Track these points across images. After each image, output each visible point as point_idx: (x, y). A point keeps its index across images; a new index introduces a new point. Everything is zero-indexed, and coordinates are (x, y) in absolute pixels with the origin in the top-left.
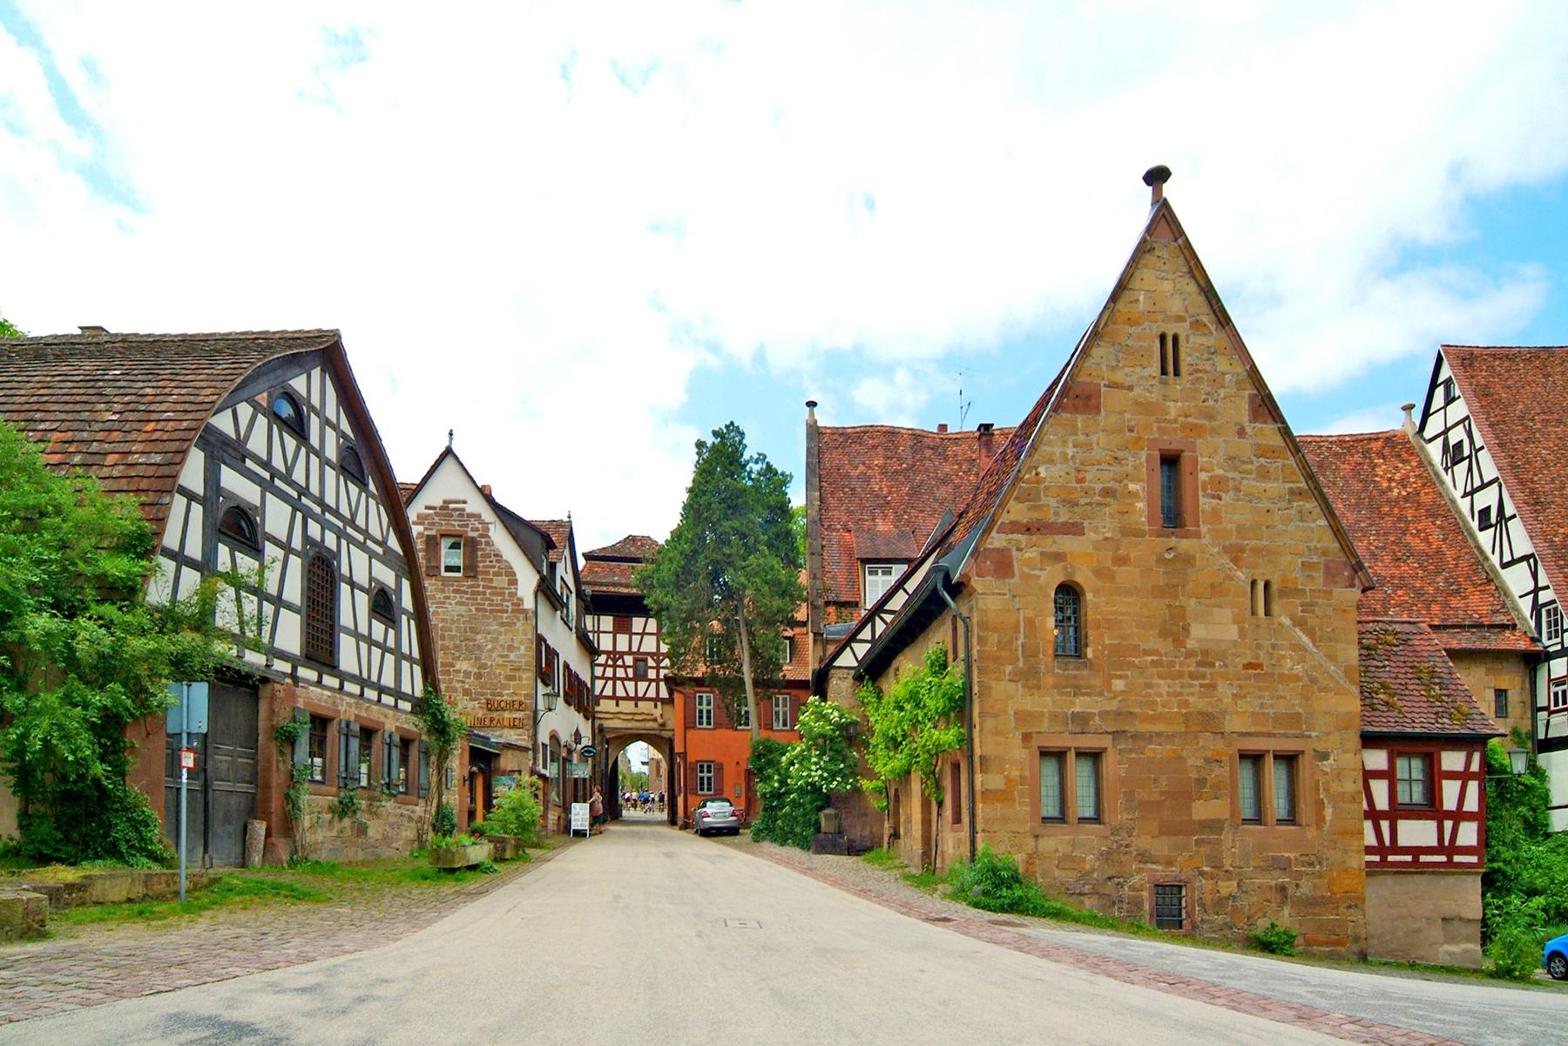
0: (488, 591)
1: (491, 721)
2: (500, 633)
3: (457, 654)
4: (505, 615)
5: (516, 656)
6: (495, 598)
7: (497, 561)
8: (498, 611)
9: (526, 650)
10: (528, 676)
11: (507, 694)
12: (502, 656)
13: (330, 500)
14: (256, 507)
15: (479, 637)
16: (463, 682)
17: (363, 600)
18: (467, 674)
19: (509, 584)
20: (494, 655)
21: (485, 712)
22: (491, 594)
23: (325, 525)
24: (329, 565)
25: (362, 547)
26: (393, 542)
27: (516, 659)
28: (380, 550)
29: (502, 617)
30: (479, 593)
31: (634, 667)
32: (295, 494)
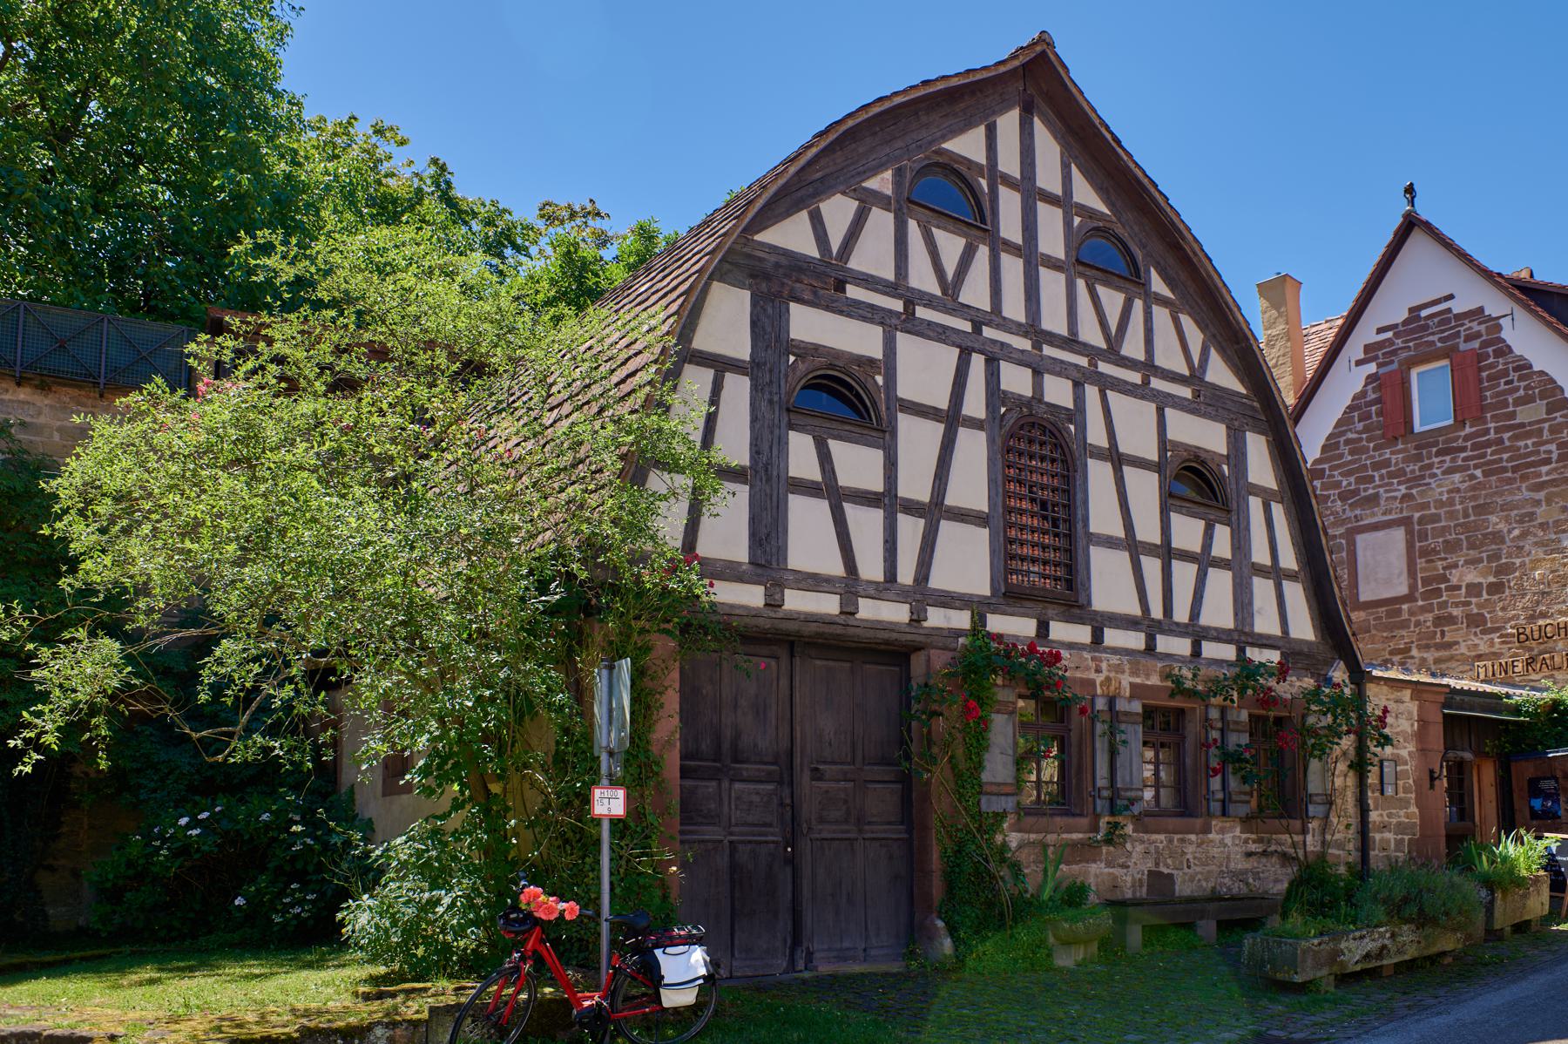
0: (1506, 436)
2: (1538, 503)
4: (1544, 469)
6: (1522, 443)
7: (1521, 379)
15: (1493, 519)
16: (1468, 604)
18: (1474, 589)
19: (1547, 414)
20: (1528, 544)
30: (1488, 444)
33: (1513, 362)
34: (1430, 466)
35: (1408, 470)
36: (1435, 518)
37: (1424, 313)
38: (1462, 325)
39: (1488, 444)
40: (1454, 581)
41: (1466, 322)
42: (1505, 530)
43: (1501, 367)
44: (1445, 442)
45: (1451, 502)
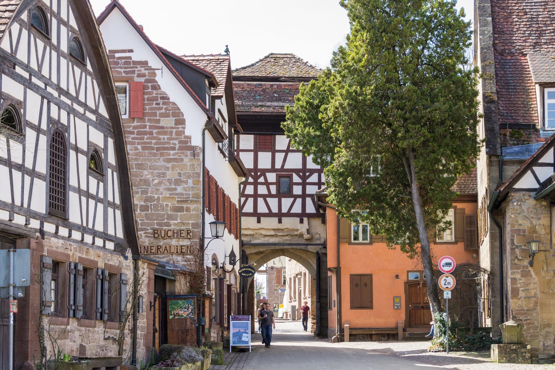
0: (155, 131)
2: (168, 168)
4: (172, 152)
6: (162, 137)
7: (163, 104)
9: (194, 184)
10: (197, 207)
12: (169, 189)
13: (63, 86)
14: (21, 102)
15: (145, 172)
17: (83, 160)
19: (176, 124)
20: (161, 189)
23: (60, 106)
24: (63, 138)
25: (83, 117)
26: (103, 111)
27: (184, 192)
28: (93, 117)
30: (145, 133)
31: (278, 184)
32: (42, 85)
33: (161, 94)
37: (117, 55)
38: (137, 68)
39: (145, 133)
41: (139, 66)
42: (151, 179)
43: (154, 95)
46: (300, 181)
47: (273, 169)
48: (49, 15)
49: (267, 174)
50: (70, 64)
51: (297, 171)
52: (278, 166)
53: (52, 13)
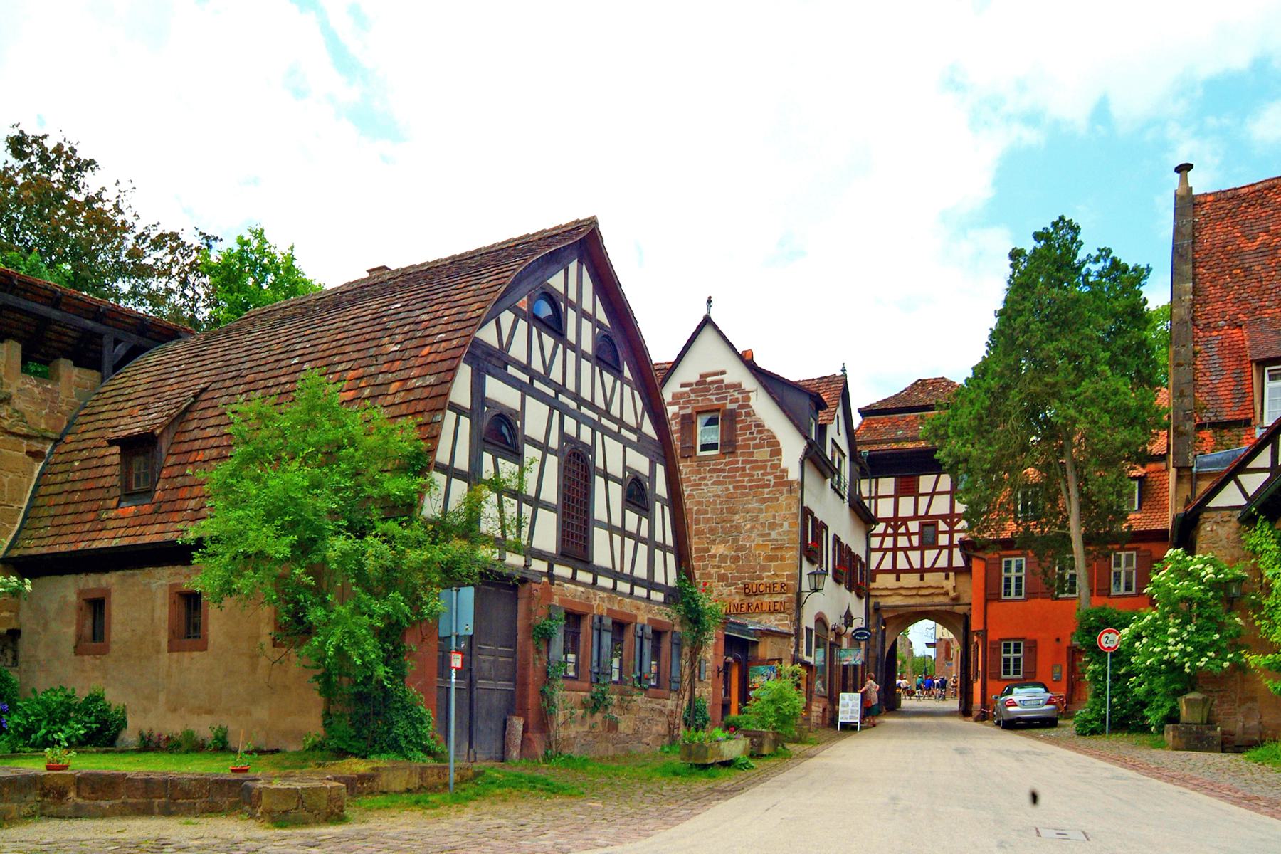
0: (748, 466)
1: (749, 607)
2: (760, 510)
3: (713, 538)
4: (766, 490)
5: (779, 534)
6: (755, 473)
7: (758, 432)
8: (758, 487)
11: (768, 577)
12: (762, 536)
13: (586, 394)
14: (517, 412)
15: (737, 516)
16: (719, 567)
17: (616, 491)
18: (723, 558)
20: (753, 535)
21: (743, 597)
22: (751, 469)
23: (580, 420)
24: (584, 460)
25: (617, 436)
26: (648, 428)
27: (779, 538)
28: (633, 437)
29: (763, 493)
30: (737, 469)
31: (920, 534)
32: (552, 393)
34: (704, 478)
35: (692, 478)
36: (706, 512)
37: (709, 379)
38: (729, 392)
39: (737, 469)
40: (713, 551)
41: (732, 391)
44: (714, 465)
45: (714, 502)
46: (947, 528)
47: (915, 517)
48: (562, 304)
49: (909, 523)
50: (597, 368)
51: (943, 517)
52: (921, 512)
53: (569, 303)
